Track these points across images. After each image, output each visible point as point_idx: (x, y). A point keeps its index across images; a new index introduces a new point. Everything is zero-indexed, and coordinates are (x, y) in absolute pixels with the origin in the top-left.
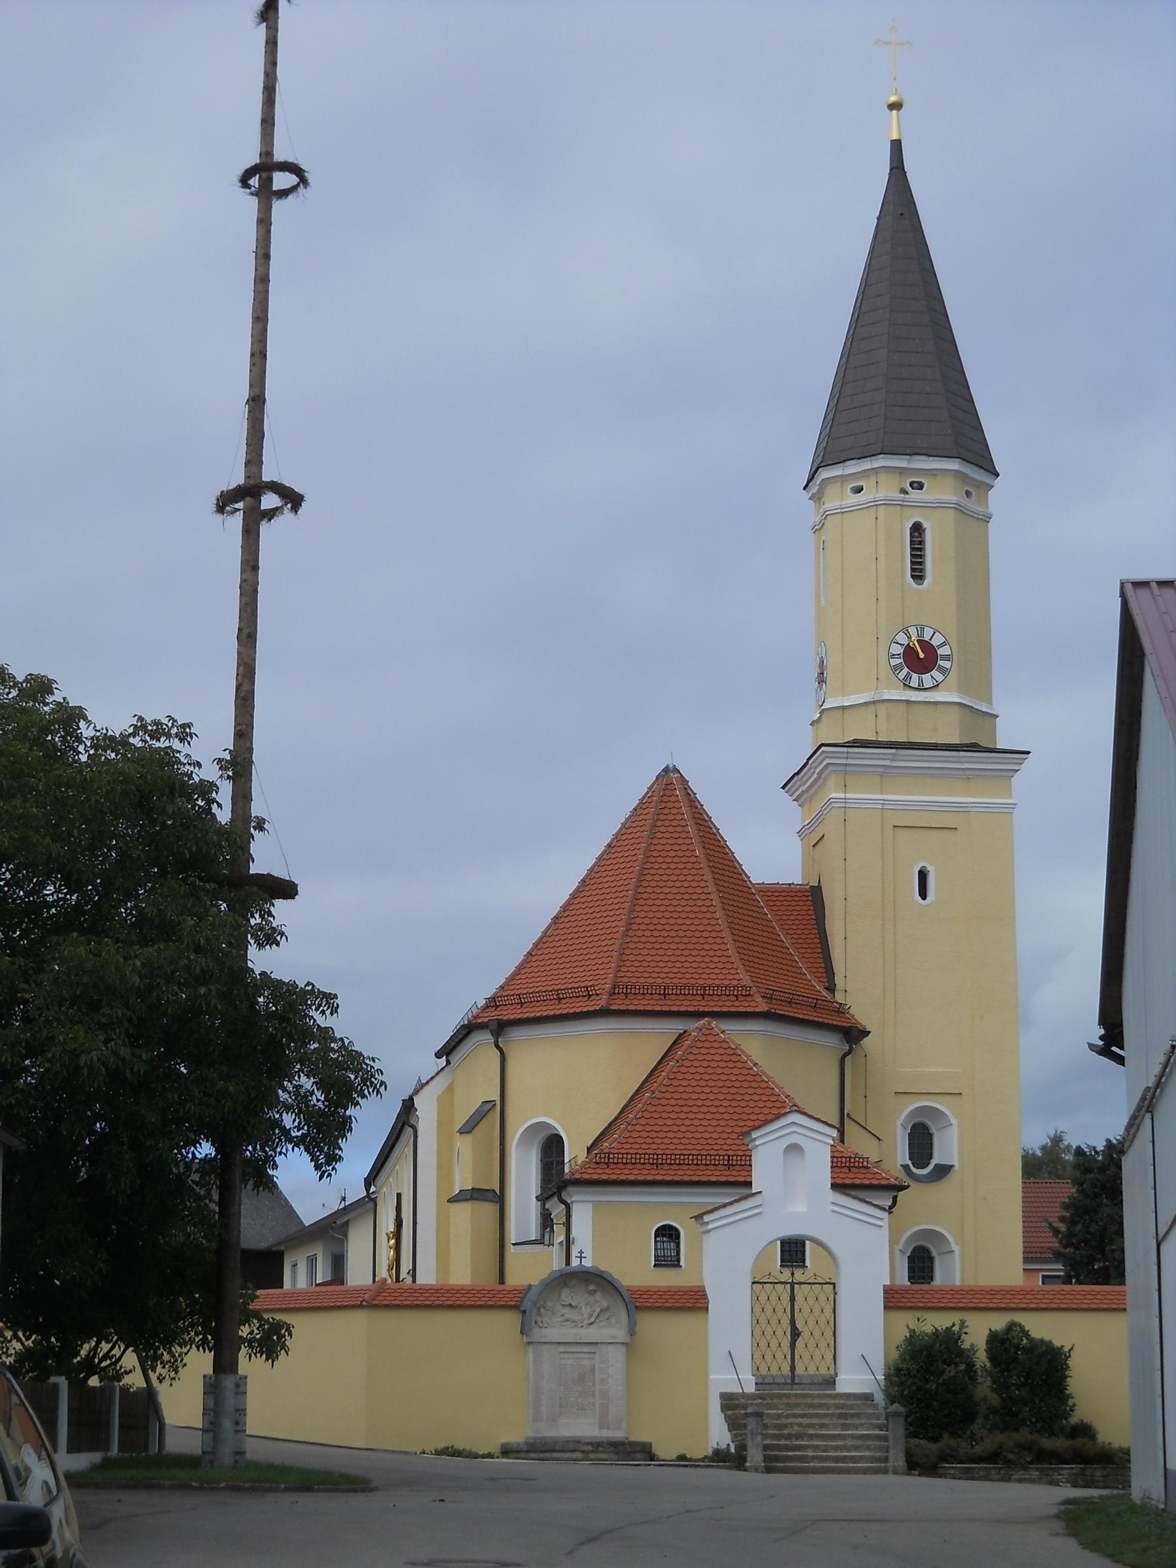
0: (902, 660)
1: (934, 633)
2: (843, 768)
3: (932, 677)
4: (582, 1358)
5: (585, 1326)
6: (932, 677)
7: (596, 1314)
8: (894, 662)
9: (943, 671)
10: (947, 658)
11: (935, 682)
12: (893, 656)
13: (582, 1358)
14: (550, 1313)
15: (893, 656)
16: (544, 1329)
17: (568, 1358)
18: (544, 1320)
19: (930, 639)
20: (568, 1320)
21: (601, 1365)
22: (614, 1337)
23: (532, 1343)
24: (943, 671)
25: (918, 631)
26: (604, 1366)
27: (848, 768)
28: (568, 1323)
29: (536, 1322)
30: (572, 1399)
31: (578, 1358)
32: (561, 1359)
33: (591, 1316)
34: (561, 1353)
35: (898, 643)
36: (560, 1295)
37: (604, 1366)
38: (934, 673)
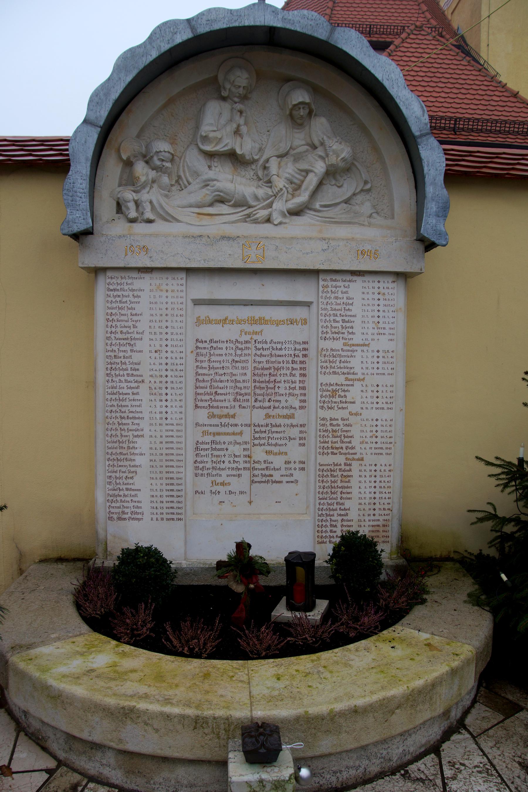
4: (262, 321)
5: (277, 218)
7: (312, 181)
13: (262, 321)
14: (165, 179)
16: (140, 228)
17: (224, 321)
18: (145, 196)
20: (221, 201)
21: (323, 344)
22: (375, 255)
23: (104, 270)
26: (338, 345)
28: (224, 209)
29: (119, 207)
30: (237, 450)
31: (253, 321)
32: (199, 322)
33: (297, 188)
34: (197, 302)
36: (197, 127)
37: (338, 345)
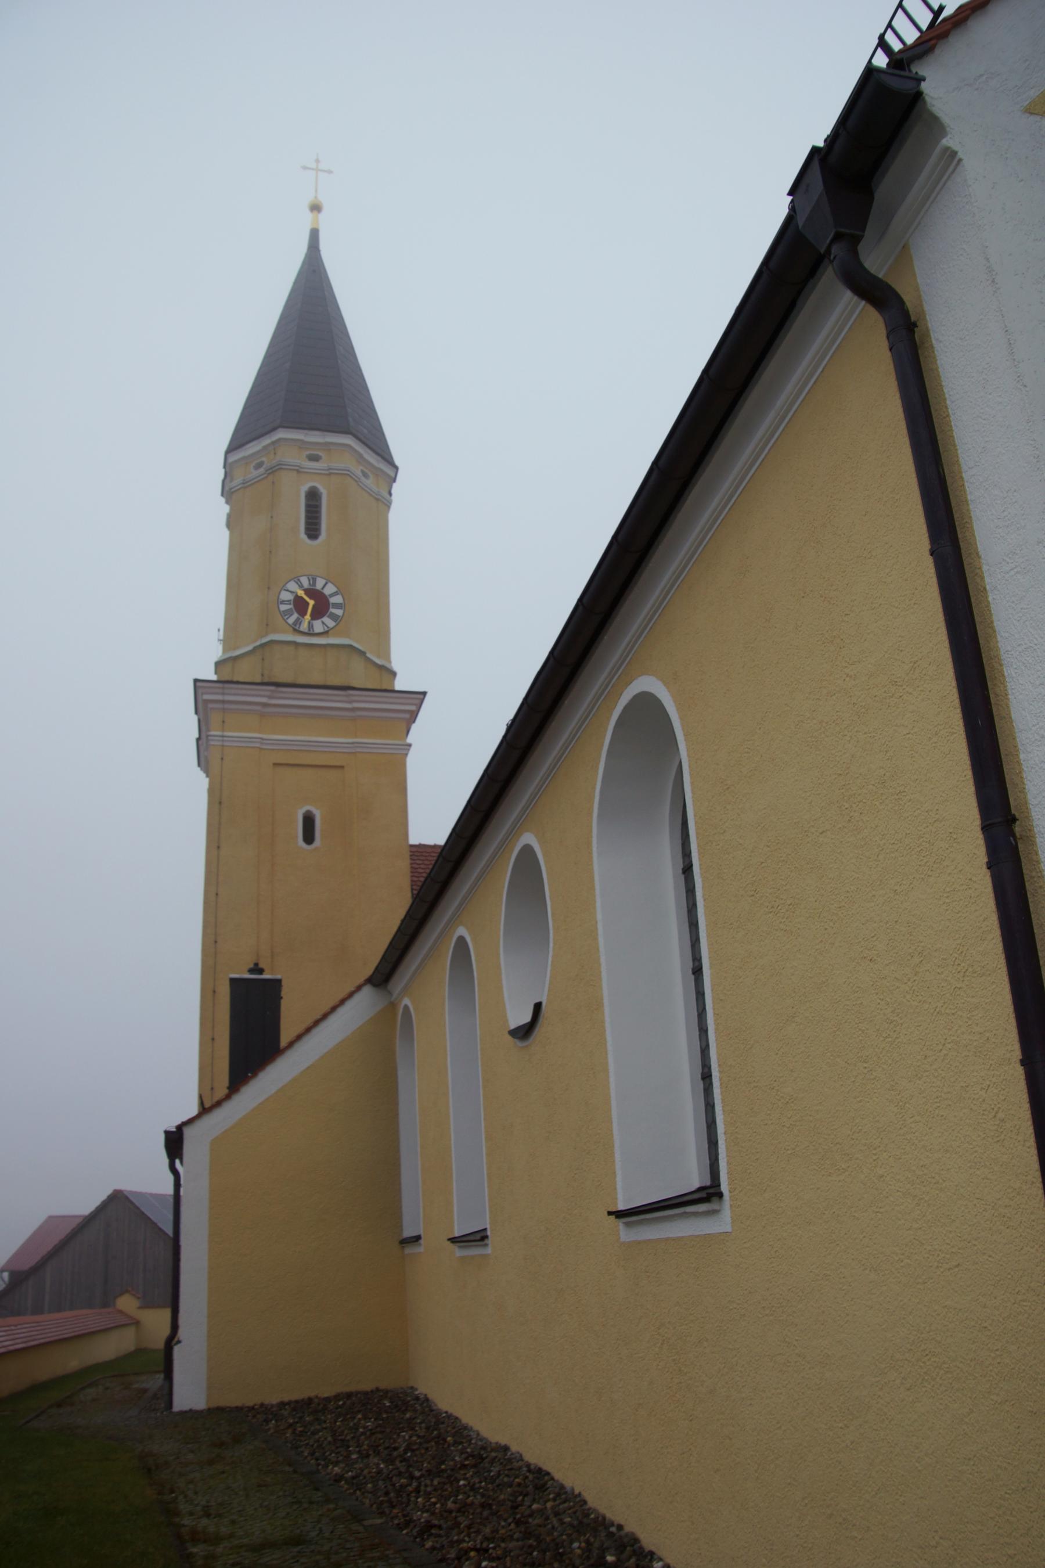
0: (291, 606)
1: (326, 584)
2: (220, 706)
3: (323, 623)
6: (323, 623)
8: (283, 607)
9: (334, 617)
10: (337, 606)
11: (326, 628)
12: (283, 602)
15: (283, 602)
19: (323, 588)
24: (334, 617)
25: (309, 580)
27: (226, 706)
35: (287, 590)
38: (326, 619)
